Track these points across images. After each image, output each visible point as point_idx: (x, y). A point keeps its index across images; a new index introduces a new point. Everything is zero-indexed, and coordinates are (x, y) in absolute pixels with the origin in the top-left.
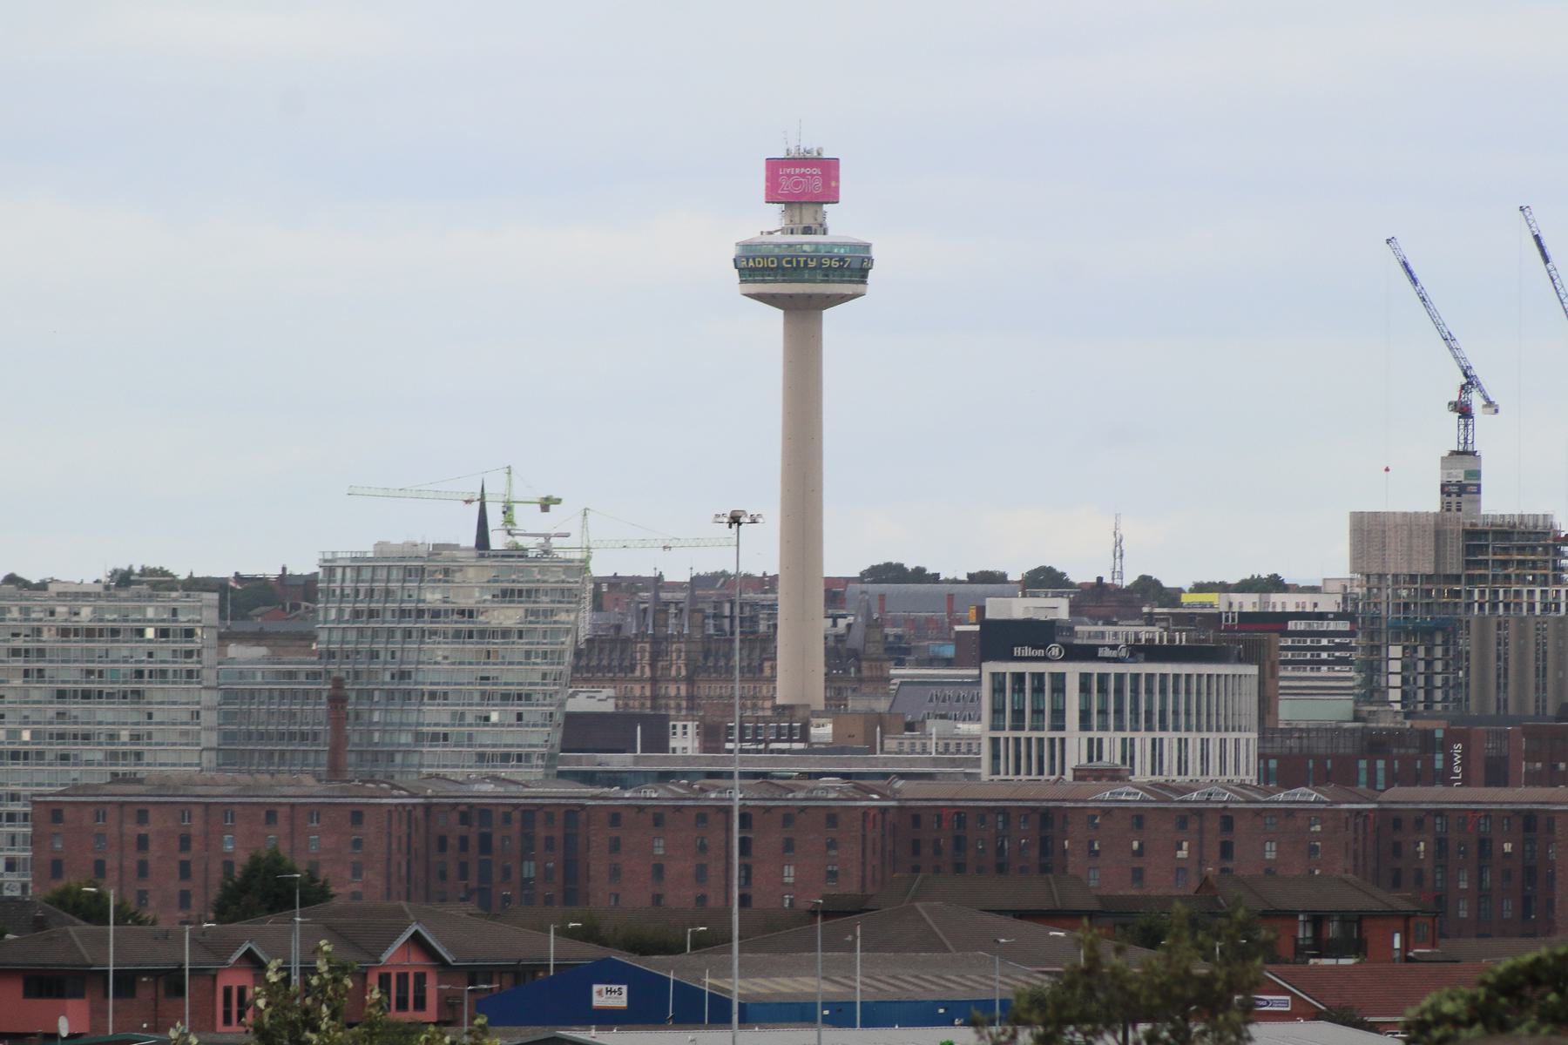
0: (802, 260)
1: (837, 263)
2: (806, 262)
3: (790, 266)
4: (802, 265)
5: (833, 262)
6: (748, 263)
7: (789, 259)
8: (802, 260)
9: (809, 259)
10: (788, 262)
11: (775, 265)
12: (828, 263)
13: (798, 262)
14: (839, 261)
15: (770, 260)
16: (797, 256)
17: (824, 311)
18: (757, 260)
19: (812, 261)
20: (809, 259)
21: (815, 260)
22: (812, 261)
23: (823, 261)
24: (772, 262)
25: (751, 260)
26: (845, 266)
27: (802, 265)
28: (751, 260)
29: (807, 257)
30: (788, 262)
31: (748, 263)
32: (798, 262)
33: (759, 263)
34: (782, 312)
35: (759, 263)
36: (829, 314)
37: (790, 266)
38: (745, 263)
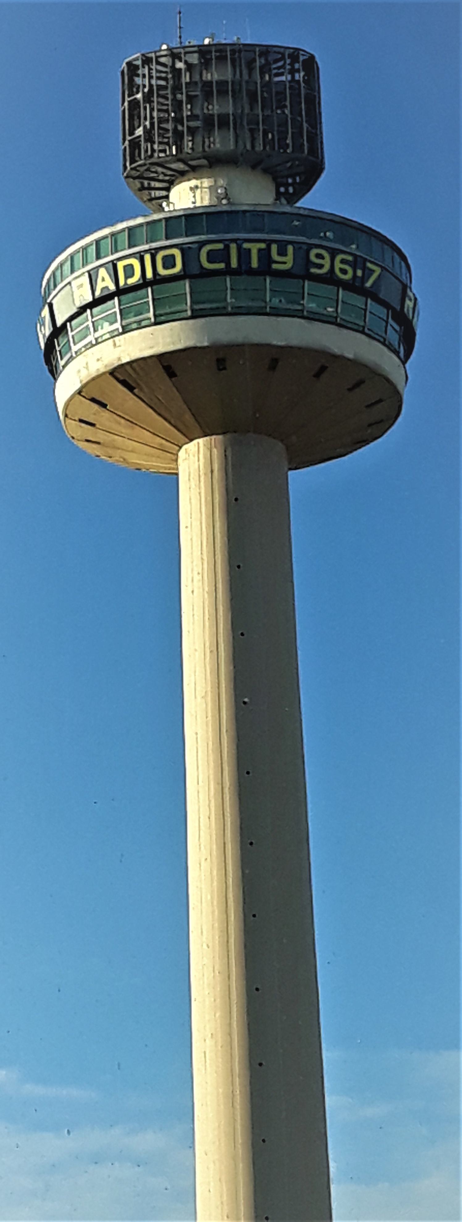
0: (254, 248)
1: (350, 271)
2: (264, 255)
3: (222, 266)
4: (255, 264)
5: (338, 265)
7: (220, 246)
8: (254, 248)
9: (274, 248)
13: (244, 255)
18: (120, 265)
19: (282, 252)
20: (274, 248)
21: (290, 249)
22: (282, 252)
24: (169, 262)
25: (103, 272)
26: (368, 284)
27: (255, 264)
28: (103, 272)
29: (269, 242)
30: (212, 257)
32: (244, 255)
33: (129, 271)
37: (222, 266)
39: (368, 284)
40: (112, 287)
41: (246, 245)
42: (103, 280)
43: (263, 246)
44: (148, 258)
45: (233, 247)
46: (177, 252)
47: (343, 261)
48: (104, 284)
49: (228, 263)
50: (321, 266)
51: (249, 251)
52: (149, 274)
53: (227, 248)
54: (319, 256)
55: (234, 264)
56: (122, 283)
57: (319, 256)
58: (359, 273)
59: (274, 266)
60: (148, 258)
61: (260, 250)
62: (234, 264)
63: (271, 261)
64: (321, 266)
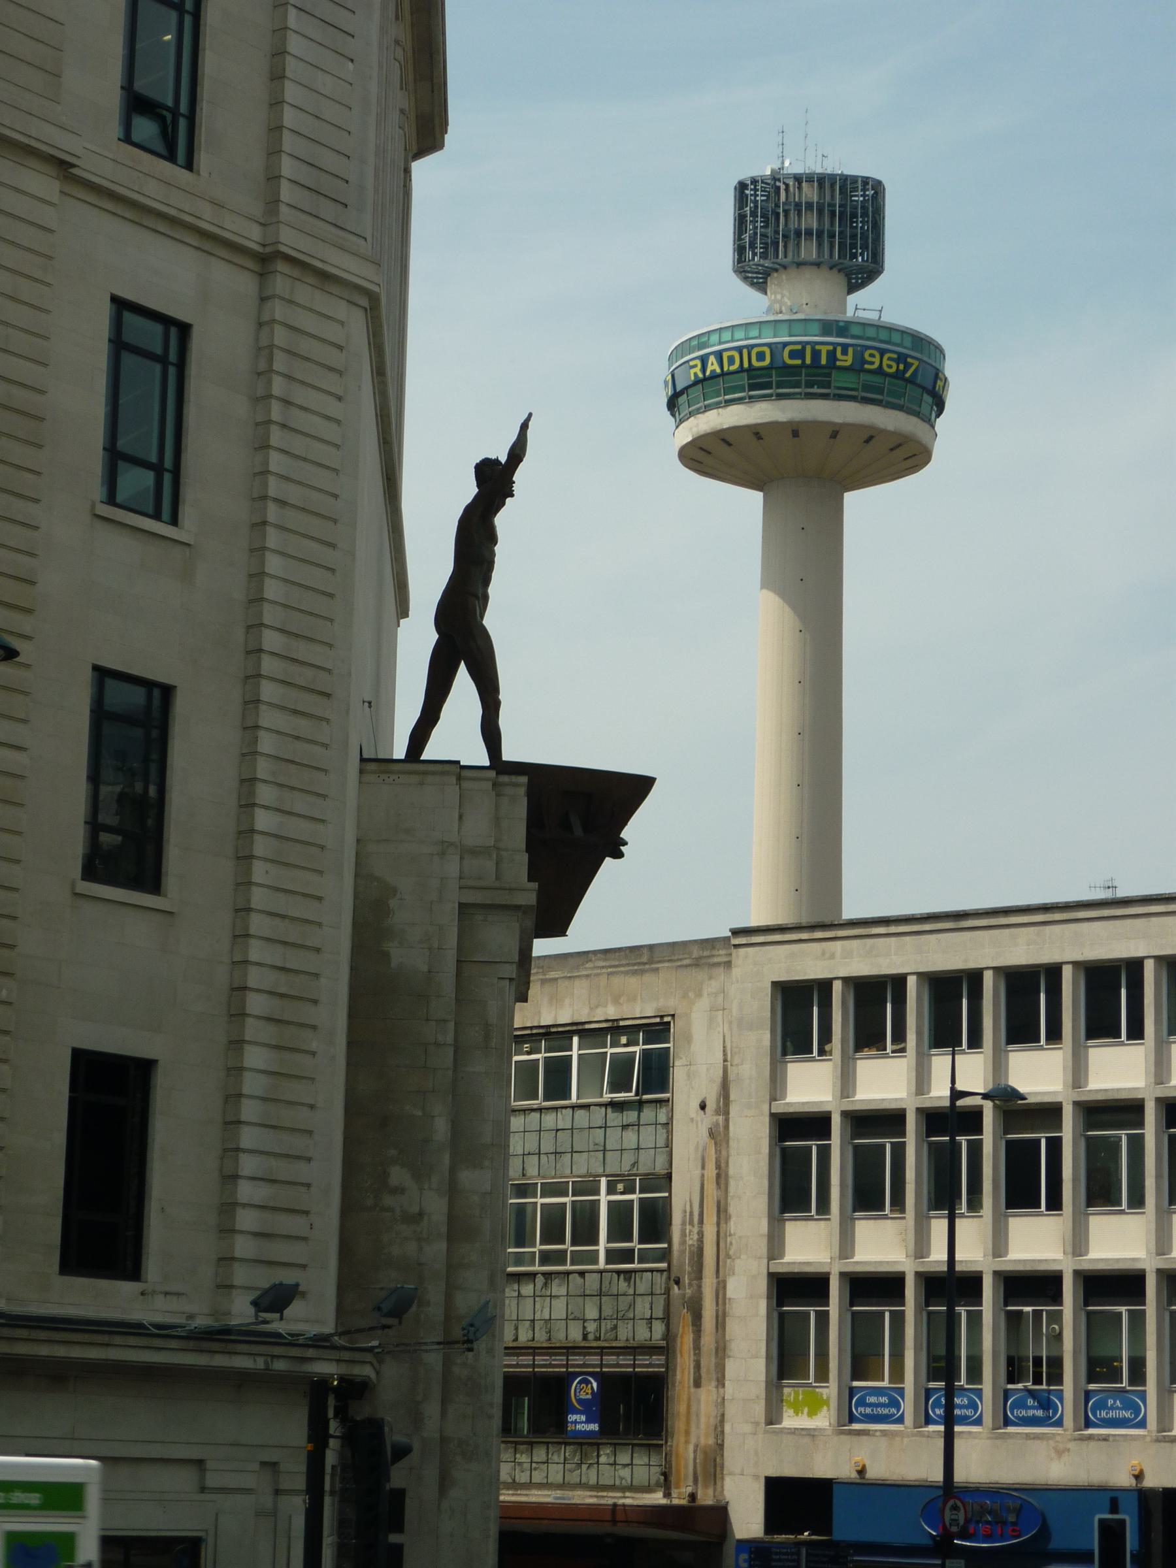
0: (824, 350)
3: (798, 362)
4: (824, 362)
5: (885, 362)
6: (704, 369)
7: (799, 347)
8: (824, 350)
9: (839, 349)
10: (793, 355)
12: (877, 360)
14: (898, 361)
17: (848, 496)
18: (725, 355)
19: (845, 352)
20: (839, 349)
21: (850, 350)
22: (845, 352)
24: (761, 356)
25: (712, 359)
26: (908, 375)
27: (824, 362)
28: (712, 359)
29: (835, 345)
31: (704, 369)
33: (731, 360)
34: (758, 496)
35: (731, 360)
37: (798, 362)
38: (698, 370)
39: (908, 375)
40: (718, 371)
41: (818, 347)
42: (712, 364)
43: (831, 348)
44: (745, 352)
45: (808, 349)
47: (889, 359)
48: (713, 368)
49: (804, 360)
50: (873, 363)
51: (820, 351)
52: (746, 365)
53: (804, 349)
54: (872, 355)
55: (808, 361)
56: (726, 369)
57: (872, 355)
58: (901, 367)
59: (838, 363)
60: (745, 352)
61: (828, 351)
62: (808, 361)
63: (835, 359)
64: (873, 363)
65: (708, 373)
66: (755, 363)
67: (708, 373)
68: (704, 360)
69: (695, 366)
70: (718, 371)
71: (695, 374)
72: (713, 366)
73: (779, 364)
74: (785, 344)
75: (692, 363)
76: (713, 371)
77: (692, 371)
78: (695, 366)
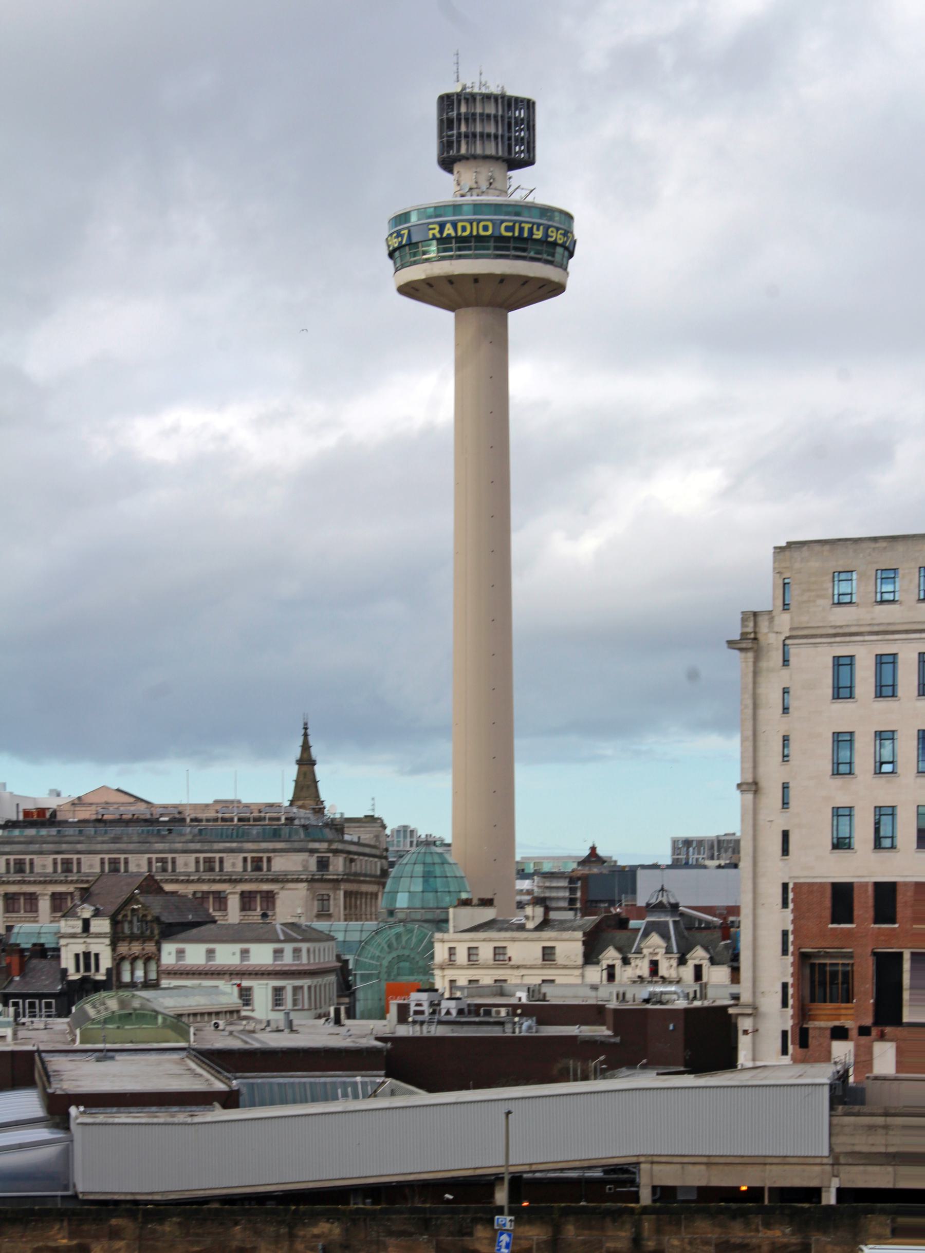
0: (527, 227)
2: (531, 230)
4: (526, 235)
5: (559, 236)
7: (511, 224)
8: (527, 227)
9: (535, 227)
10: (507, 229)
11: (489, 233)
13: (521, 230)
15: (481, 224)
16: (521, 222)
17: (514, 316)
18: (460, 225)
20: (535, 227)
21: (541, 228)
22: (538, 230)
23: (550, 233)
24: (486, 228)
27: (526, 235)
28: (448, 226)
29: (533, 224)
30: (507, 229)
33: (464, 229)
35: (464, 229)
36: (517, 319)
37: (510, 234)
38: (436, 232)
41: (523, 225)
42: (449, 229)
43: (530, 226)
44: (475, 224)
46: (490, 225)
48: (449, 232)
49: (514, 232)
50: (552, 237)
53: (514, 226)
56: (459, 233)
57: (552, 232)
58: (565, 239)
59: (534, 237)
60: (475, 224)
62: (517, 234)
64: (552, 237)
65: (445, 235)
66: (482, 233)
67: (445, 235)
68: (442, 226)
69: (434, 229)
70: (453, 234)
71: (434, 235)
72: (449, 230)
73: (497, 234)
74: (502, 221)
75: (431, 226)
76: (449, 235)
77: (431, 232)
78: (434, 229)
